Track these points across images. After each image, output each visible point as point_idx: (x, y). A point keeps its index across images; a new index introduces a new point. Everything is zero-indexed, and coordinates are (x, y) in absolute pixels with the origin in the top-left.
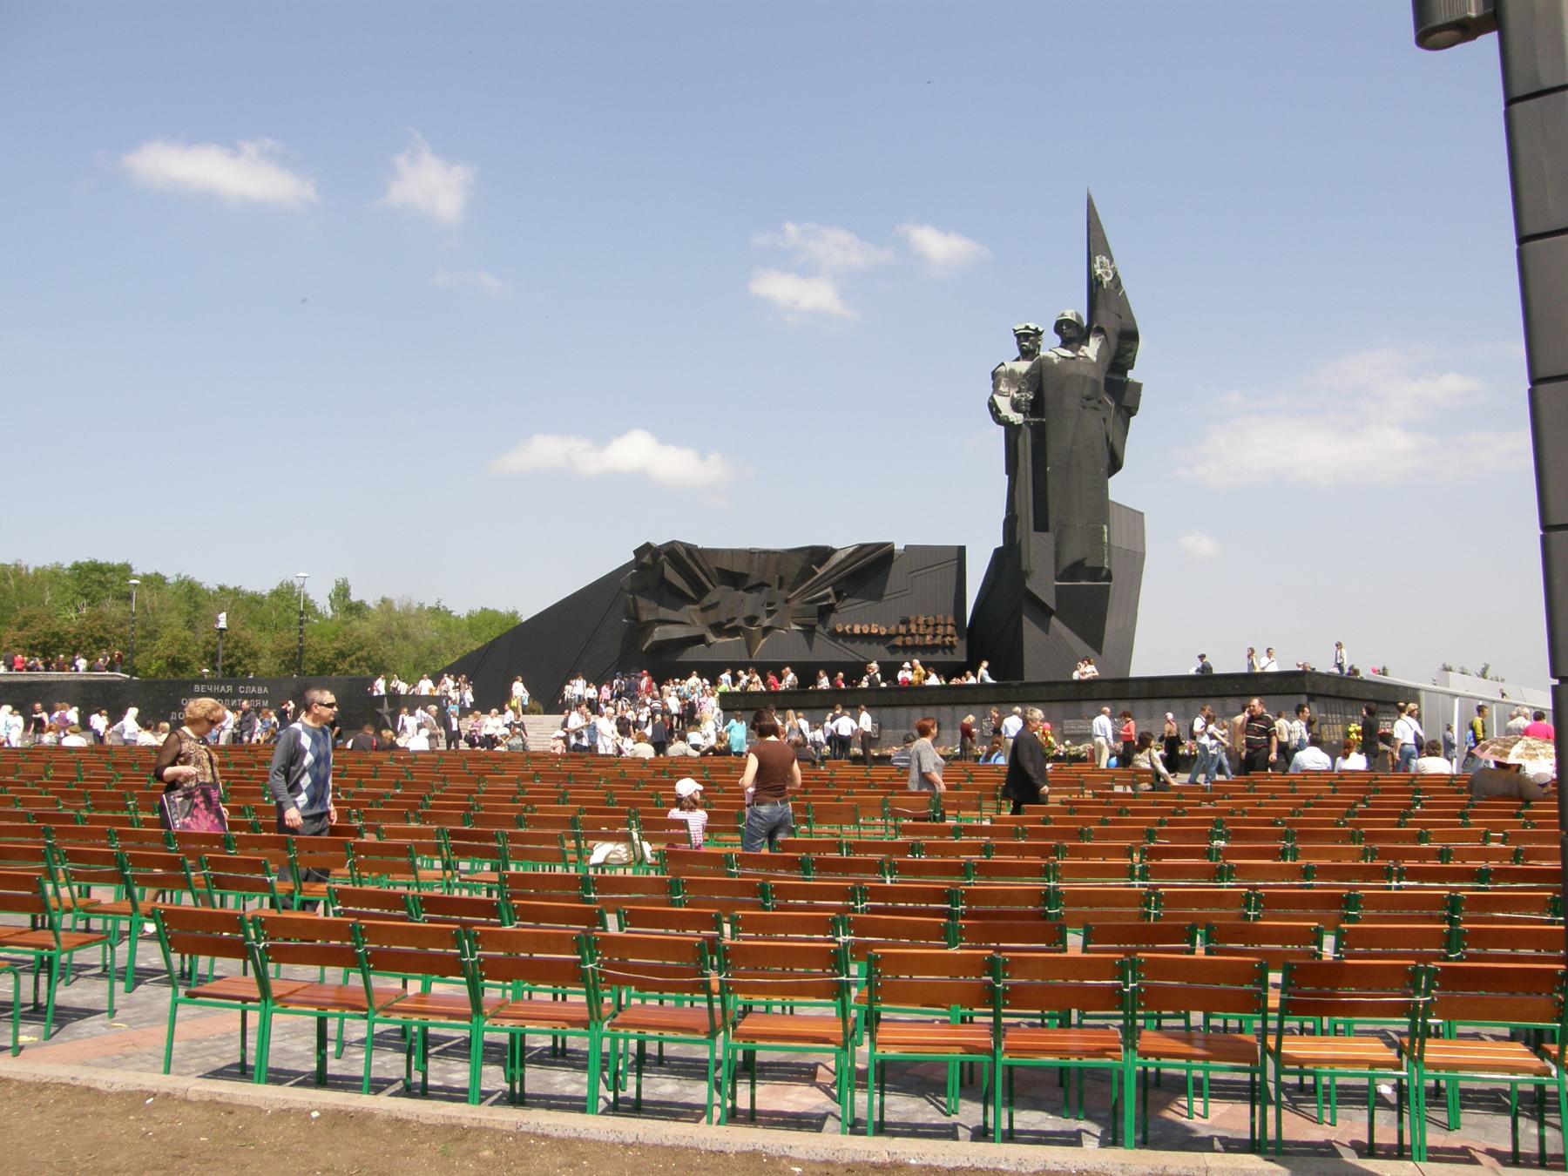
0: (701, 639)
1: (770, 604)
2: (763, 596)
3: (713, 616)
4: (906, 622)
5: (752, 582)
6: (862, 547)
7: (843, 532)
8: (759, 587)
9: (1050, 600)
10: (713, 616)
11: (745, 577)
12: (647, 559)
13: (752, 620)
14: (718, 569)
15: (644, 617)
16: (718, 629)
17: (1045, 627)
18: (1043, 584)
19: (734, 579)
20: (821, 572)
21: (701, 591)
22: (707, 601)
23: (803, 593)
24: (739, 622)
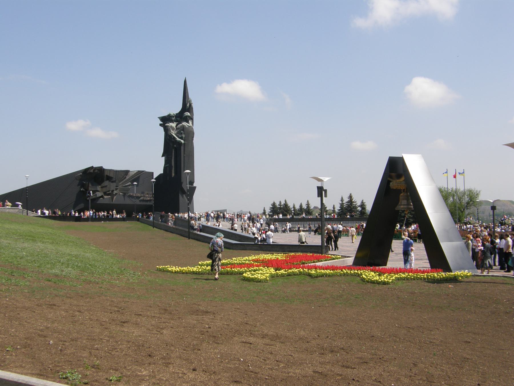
0: (102, 197)
1: (116, 187)
3: (105, 190)
4: (143, 193)
5: (114, 180)
6: (139, 171)
7: (133, 167)
8: (115, 182)
10: (105, 190)
11: (112, 178)
12: (92, 171)
13: (113, 191)
14: (107, 175)
16: (105, 194)
19: (109, 178)
20: (127, 178)
21: (103, 181)
23: (123, 183)
24: (111, 192)
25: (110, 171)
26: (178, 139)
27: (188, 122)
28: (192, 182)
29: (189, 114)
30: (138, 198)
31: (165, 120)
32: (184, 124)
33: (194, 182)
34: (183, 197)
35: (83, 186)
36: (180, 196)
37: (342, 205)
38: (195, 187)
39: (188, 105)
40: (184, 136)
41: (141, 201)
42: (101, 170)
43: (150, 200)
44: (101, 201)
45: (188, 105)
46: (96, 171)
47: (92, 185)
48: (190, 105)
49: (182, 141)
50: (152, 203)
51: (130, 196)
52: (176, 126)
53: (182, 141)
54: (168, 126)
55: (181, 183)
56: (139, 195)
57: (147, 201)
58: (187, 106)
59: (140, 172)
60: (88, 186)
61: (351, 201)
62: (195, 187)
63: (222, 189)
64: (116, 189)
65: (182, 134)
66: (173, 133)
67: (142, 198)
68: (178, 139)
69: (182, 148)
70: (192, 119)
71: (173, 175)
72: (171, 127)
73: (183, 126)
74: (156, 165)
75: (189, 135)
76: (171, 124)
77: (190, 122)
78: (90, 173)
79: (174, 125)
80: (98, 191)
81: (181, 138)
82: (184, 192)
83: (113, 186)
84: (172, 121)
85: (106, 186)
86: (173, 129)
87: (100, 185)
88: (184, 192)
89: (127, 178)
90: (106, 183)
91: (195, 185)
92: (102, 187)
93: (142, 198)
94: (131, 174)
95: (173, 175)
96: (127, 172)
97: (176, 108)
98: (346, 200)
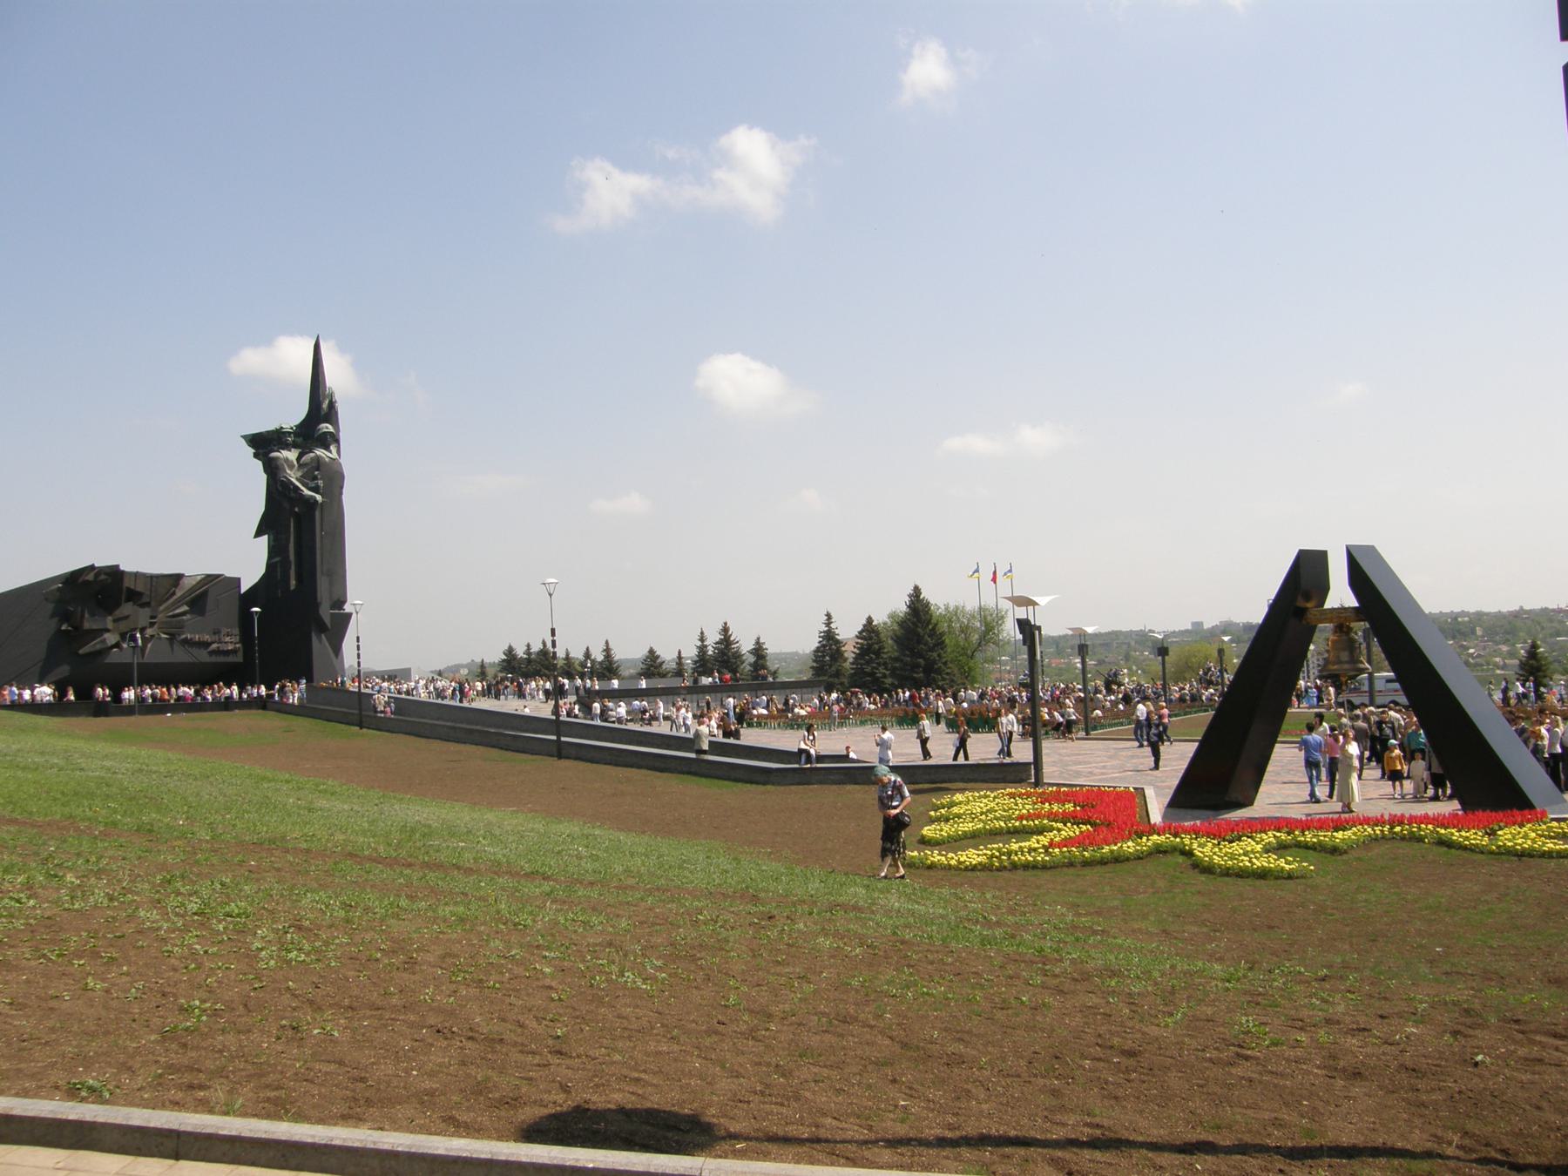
0: (117, 645)
2: (147, 611)
3: (123, 626)
5: (146, 599)
8: (147, 604)
9: (327, 621)
10: (123, 626)
11: (140, 594)
12: (90, 577)
14: (129, 589)
15: (87, 625)
17: (320, 641)
18: (326, 612)
19: (133, 596)
20: (179, 594)
21: (118, 605)
22: (119, 613)
23: (167, 608)
25: (137, 575)
26: (307, 492)
27: (327, 448)
28: (340, 603)
29: (331, 429)
30: (208, 644)
31: (263, 444)
32: (320, 452)
33: (344, 602)
34: (320, 641)
35: (65, 617)
36: (314, 638)
37: (702, 649)
38: (349, 616)
39: (325, 405)
40: (320, 483)
41: (212, 653)
42: (114, 573)
43: (234, 651)
44: (115, 657)
45: (325, 405)
46: (103, 577)
47: (93, 615)
48: (332, 405)
49: (319, 498)
50: (239, 658)
51: (186, 642)
52: (298, 459)
53: (319, 498)
54: (277, 459)
55: (315, 605)
56: (207, 638)
57: (227, 653)
58: (321, 408)
59: (210, 579)
60: (83, 616)
61: (726, 640)
62: (349, 616)
63: (407, 616)
64: (152, 625)
65: (315, 478)
66: (293, 476)
67: (214, 646)
68: (307, 492)
69: (317, 514)
70: (337, 441)
71: (293, 582)
72: (287, 460)
73: (318, 458)
74: (247, 561)
75: (330, 479)
76: (285, 454)
77: (333, 448)
78: (87, 583)
79: (291, 455)
80: (108, 631)
81: (316, 489)
82: (322, 628)
83: (143, 616)
84: (287, 447)
85: (127, 617)
86: (291, 466)
87: (110, 614)
88: (322, 628)
89: (179, 594)
90: (127, 609)
91: (348, 608)
92: (115, 621)
93: (214, 646)
94: (187, 584)
95: (293, 582)
96: (178, 578)
97: (292, 414)
98: (713, 638)
